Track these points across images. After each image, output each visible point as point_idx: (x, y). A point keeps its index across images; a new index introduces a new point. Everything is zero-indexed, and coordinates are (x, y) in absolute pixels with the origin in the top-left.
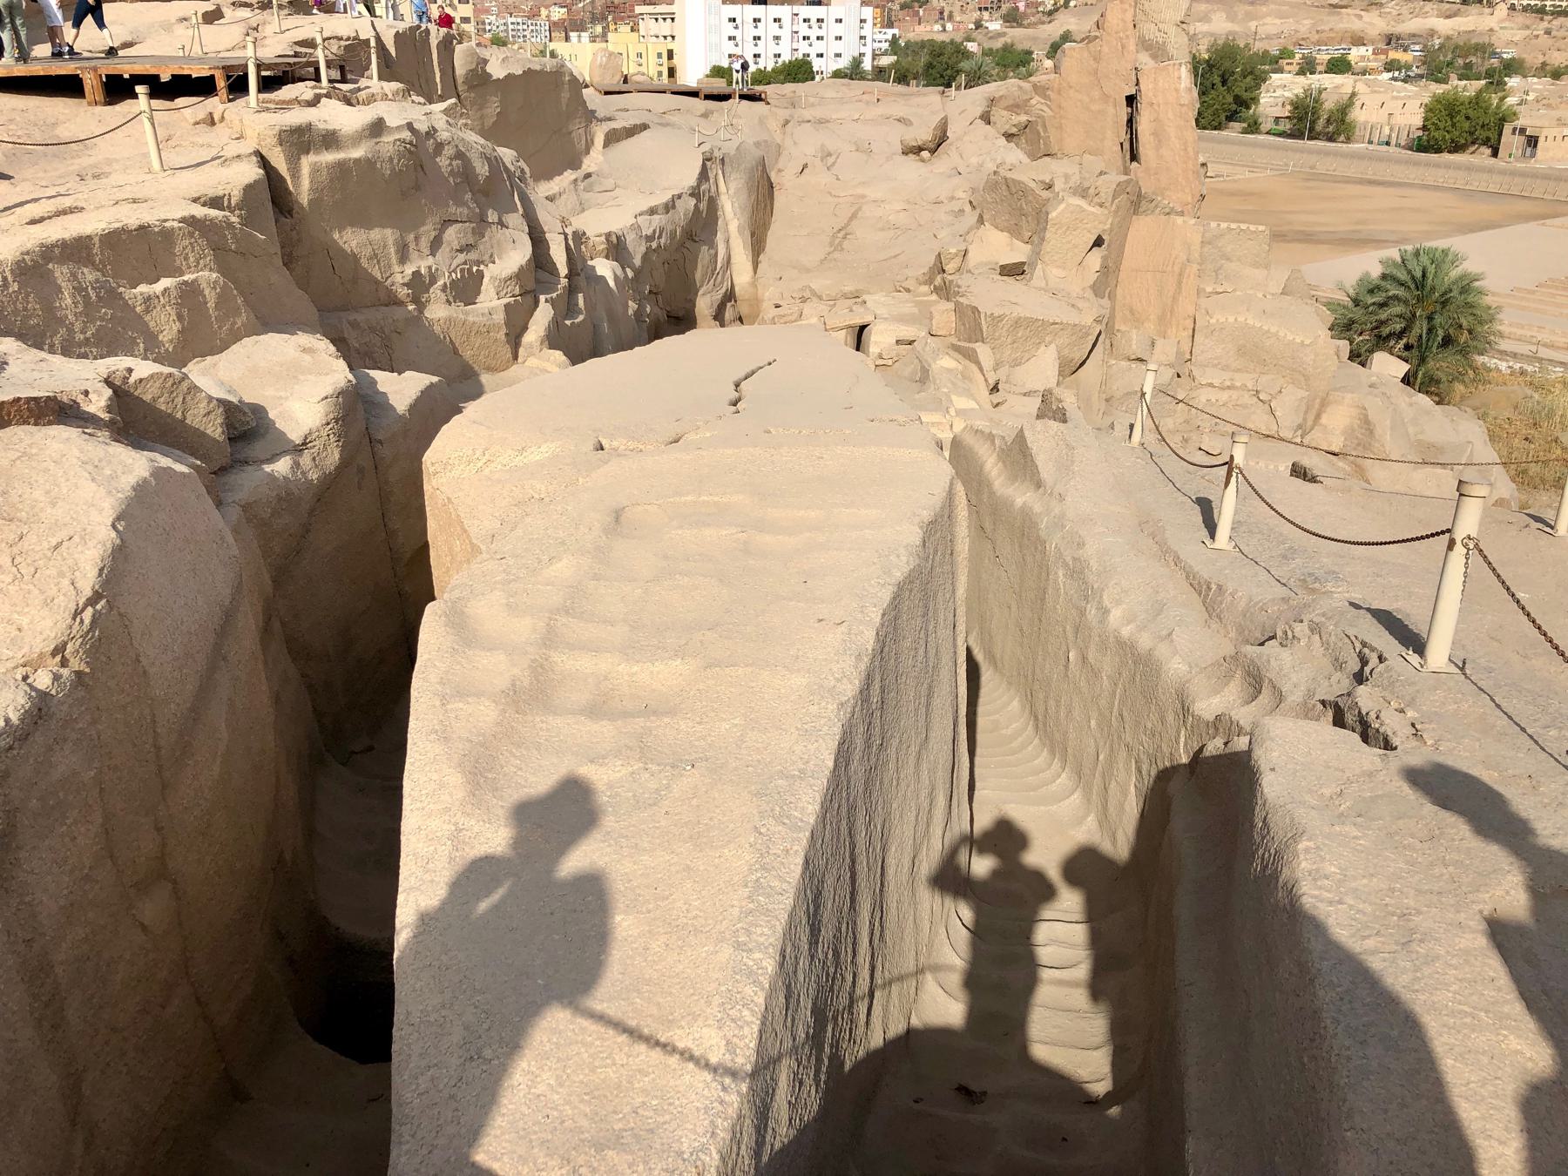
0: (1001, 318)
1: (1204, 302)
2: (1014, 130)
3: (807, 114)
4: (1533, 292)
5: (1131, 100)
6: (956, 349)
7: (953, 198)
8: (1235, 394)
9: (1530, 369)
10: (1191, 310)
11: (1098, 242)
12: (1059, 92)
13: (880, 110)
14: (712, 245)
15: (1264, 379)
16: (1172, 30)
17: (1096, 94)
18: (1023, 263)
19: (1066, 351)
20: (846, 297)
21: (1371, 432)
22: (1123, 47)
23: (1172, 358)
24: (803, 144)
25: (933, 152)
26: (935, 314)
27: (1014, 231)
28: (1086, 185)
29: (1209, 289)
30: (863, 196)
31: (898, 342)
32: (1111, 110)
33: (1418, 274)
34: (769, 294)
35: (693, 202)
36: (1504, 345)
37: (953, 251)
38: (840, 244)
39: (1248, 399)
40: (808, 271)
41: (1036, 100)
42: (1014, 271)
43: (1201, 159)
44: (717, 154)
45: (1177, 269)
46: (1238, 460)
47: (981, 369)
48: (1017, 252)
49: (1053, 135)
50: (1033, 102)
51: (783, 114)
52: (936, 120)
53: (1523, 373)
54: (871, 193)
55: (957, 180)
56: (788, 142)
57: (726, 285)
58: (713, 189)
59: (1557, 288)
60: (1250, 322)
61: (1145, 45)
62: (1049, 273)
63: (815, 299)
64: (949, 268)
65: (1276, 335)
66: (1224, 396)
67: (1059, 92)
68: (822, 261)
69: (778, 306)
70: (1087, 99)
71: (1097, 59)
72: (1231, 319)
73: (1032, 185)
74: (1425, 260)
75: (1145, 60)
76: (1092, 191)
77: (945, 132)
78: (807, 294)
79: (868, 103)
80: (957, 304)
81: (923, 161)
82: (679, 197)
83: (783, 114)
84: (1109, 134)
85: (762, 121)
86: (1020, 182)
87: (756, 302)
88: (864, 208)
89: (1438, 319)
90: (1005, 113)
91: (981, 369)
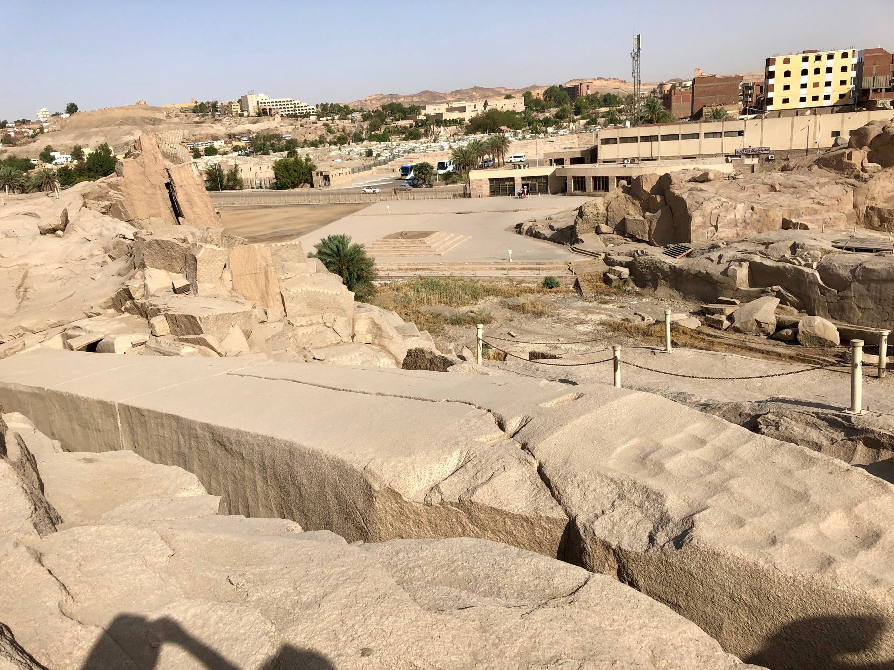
1: (283, 285)
2: (104, 210)
5: (168, 185)
6: (187, 341)
7: (92, 256)
8: (314, 327)
10: (278, 290)
12: (126, 186)
15: (325, 316)
16: (179, 147)
17: (148, 184)
18: (188, 285)
20: (51, 326)
25: (63, 230)
26: (155, 324)
27: (170, 268)
28: (205, 236)
29: (283, 278)
30: (26, 264)
33: (336, 249)
36: (381, 274)
37: (137, 286)
38: (24, 295)
39: (322, 328)
40: (11, 317)
41: (112, 192)
42: (184, 290)
43: (216, 211)
45: (263, 271)
46: (619, 358)
47: (212, 348)
49: (128, 208)
52: (60, 212)
53: (386, 285)
54: (33, 260)
55: (89, 245)
60: (309, 289)
61: (166, 156)
62: (205, 286)
63: (28, 333)
64: (136, 295)
65: (323, 293)
66: (310, 329)
67: (126, 186)
68: (18, 309)
71: (142, 165)
72: (300, 290)
74: (336, 242)
75: (168, 163)
76: (209, 239)
77: (67, 217)
78: (21, 332)
80: (166, 315)
81: (59, 236)
84: (161, 204)
86: (167, 241)
89: (351, 268)
91: (212, 348)
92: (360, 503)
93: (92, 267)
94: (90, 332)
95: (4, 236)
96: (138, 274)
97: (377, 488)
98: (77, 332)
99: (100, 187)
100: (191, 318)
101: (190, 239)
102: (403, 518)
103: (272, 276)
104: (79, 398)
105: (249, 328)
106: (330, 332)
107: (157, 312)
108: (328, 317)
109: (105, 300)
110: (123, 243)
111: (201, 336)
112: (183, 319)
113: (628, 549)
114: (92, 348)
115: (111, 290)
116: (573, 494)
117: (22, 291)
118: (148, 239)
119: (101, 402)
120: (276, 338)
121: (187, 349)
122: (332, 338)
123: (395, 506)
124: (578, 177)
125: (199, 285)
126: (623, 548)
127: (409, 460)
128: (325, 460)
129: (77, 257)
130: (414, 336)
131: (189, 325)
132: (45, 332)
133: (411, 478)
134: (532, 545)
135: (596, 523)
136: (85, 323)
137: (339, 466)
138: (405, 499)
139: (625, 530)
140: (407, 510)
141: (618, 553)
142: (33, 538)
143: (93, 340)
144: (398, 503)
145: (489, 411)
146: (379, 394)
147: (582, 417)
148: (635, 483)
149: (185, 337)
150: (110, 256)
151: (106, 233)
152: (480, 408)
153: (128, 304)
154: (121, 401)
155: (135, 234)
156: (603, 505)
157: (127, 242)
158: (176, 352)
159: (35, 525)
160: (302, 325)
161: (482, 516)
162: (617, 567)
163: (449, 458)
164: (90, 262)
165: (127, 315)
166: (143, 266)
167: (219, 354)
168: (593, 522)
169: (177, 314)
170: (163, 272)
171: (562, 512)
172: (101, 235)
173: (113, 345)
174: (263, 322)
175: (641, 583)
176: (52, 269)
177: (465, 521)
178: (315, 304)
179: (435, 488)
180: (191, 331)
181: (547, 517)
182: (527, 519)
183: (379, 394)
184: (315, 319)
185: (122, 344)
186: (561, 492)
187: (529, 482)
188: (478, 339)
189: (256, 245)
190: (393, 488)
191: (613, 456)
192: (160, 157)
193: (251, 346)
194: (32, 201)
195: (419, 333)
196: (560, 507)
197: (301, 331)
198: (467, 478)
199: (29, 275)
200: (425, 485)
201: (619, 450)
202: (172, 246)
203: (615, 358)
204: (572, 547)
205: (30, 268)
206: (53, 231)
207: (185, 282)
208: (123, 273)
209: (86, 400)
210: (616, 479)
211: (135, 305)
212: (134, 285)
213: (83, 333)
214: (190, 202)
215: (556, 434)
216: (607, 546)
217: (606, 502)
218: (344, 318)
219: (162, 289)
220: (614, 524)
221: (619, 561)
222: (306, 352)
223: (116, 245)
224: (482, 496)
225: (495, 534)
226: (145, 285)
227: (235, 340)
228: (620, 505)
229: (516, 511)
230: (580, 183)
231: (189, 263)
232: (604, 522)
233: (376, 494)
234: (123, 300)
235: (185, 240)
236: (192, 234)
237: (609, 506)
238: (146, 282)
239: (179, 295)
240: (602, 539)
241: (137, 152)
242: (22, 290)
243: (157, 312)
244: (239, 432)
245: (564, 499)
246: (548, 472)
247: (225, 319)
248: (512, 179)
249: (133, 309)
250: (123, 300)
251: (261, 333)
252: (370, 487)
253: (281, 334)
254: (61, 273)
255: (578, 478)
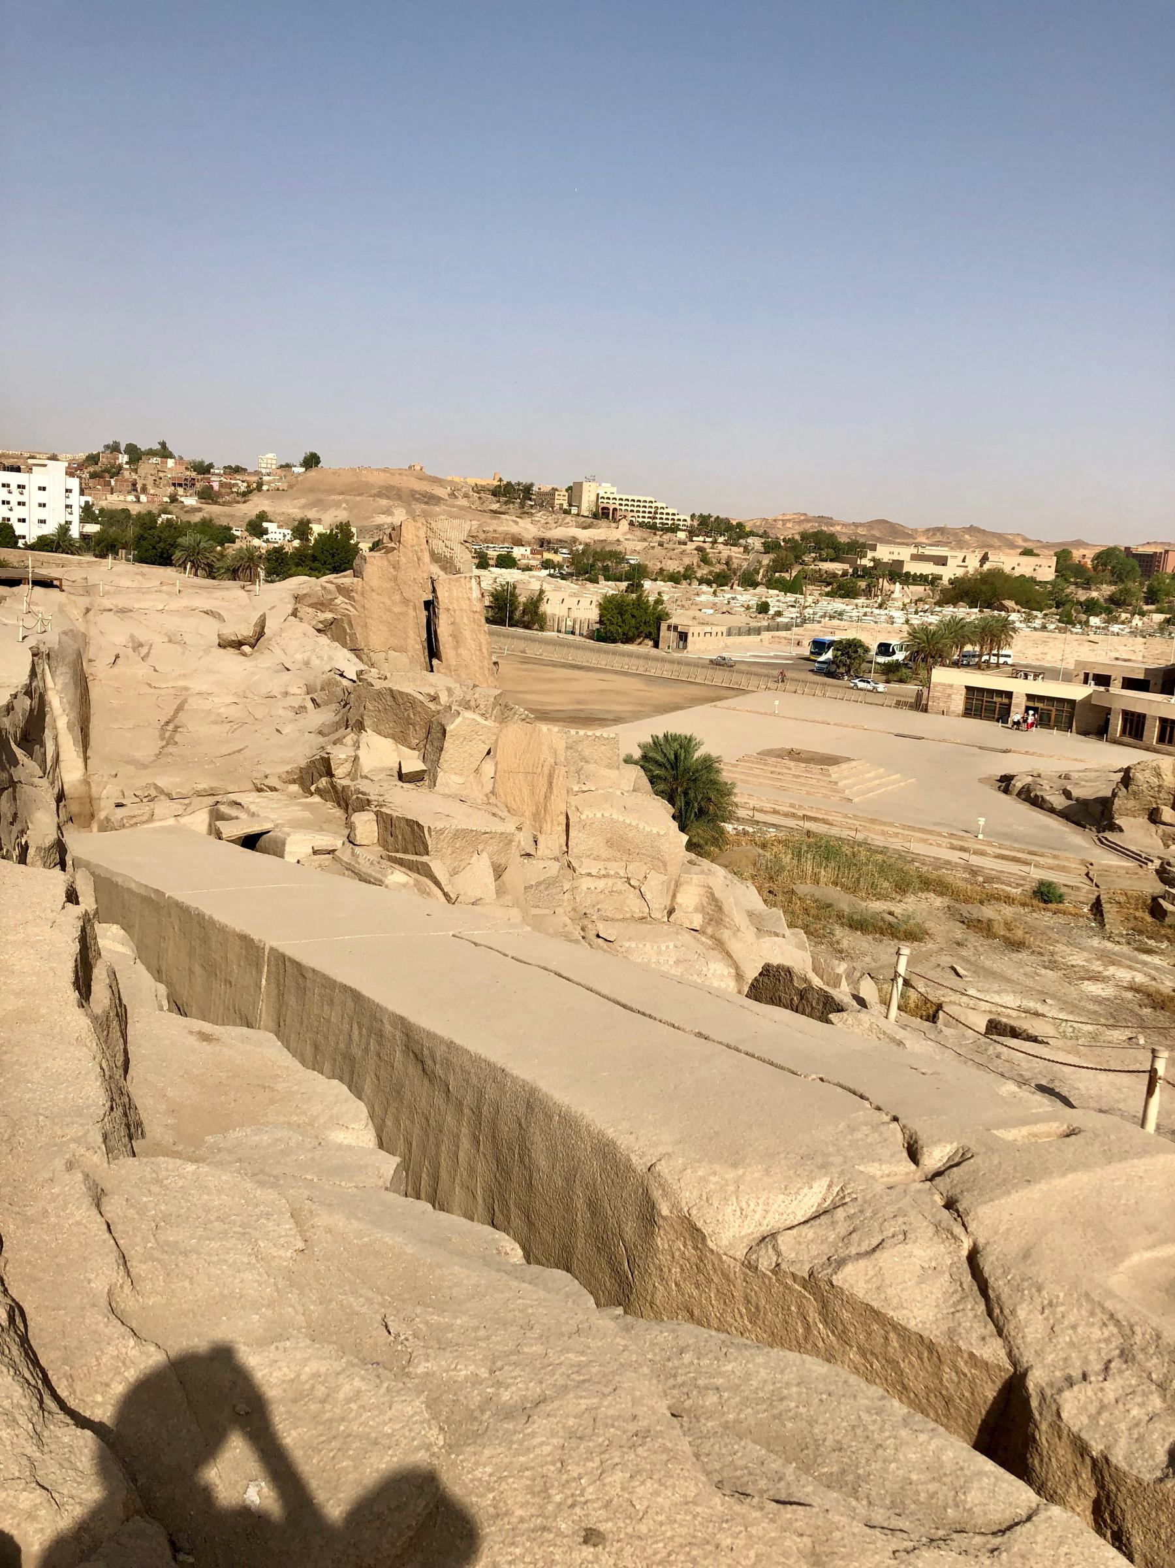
0: (442, 831)
1: (574, 800)
2: (321, 626)
3: (107, 603)
4: (736, 766)
5: (429, 605)
6: (401, 863)
7: (286, 694)
8: (610, 882)
9: (751, 830)
11: (488, 753)
12: (362, 594)
13: (177, 604)
14: (42, 744)
15: (631, 867)
17: (397, 597)
18: (424, 771)
19: (495, 858)
21: (720, 909)
22: (419, 559)
23: (557, 853)
24: (110, 635)
25: (253, 646)
27: (401, 738)
29: (576, 788)
30: (186, 689)
31: (315, 852)
32: (412, 613)
33: (673, 757)
34: (107, 793)
35: (28, 702)
37: (343, 756)
38: (172, 737)
39: (621, 885)
40: (145, 767)
41: (340, 600)
43: (494, 659)
44: (43, 649)
45: (546, 772)
46: (1161, 1072)
47: (437, 884)
48: (413, 763)
49: (358, 630)
50: (338, 601)
51: (83, 602)
52: (255, 617)
53: (745, 833)
54: (196, 685)
55: (287, 676)
56: (93, 632)
57: (58, 785)
58: (41, 685)
59: (753, 762)
61: (435, 558)
62: (449, 778)
63: (162, 797)
64: (339, 772)
65: (637, 827)
66: (601, 884)
67: (362, 594)
69: (119, 805)
70: (389, 602)
71: (396, 566)
72: (599, 815)
73: (421, 697)
74: (676, 746)
75: (436, 570)
76: (473, 703)
78: (153, 793)
79: (169, 594)
80: (377, 814)
81: (245, 655)
82: (15, 696)
83: (83, 602)
84: (411, 634)
85: (61, 609)
86: (407, 695)
87: (90, 800)
88: (190, 700)
89: (691, 794)
90: (310, 610)
91: (437, 884)
92: (630, 1229)
93: (281, 712)
94: (253, 815)
95: (166, 640)
96: (350, 738)
97: (665, 1212)
98: (233, 812)
99: (324, 588)
100: (415, 827)
101: (444, 699)
102: (701, 1278)
103: (559, 782)
104: (212, 922)
105: (503, 861)
106: (633, 895)
107: (364, 804)
108: (636, 869)
109: (288, 768)
110: (337, 684)
111: (425, 859)
112: (403, 824)
113: (1123, 1465)
114: (250, 842)
115: (301, 755)
116: (1029, 1324)
117: (170, 729)
118: (378, 685)
119: (245, 939)
120: (542, 887)
121: (398, 876)
122: (635, 906)
123: (690, 1252)
124: (1133, 714)
125: (440, 774)
126: (1113, 1460)
127: (731, 1175)
128: (584, 1134)
129: (264, 691)
130: (777, 935)
131: (409, 836)
132: (186, 801)
133: (729, 1210)
134: (933, 1399)
135: (1067, 1394)
136: (249, 798)
137: (606, 1151)
138: (709, 1243)
139: (1123, 1426)
140: (709, 1267)
141: (1100, 1468)
142: (97, 1159)
143: (255, 829)
144: (696, 1248)
145: (895, 1119)
146: (699, 1035)
147: (1070, 1176)
148: (1159, 1337)
149: (399, 855)
150: (313, 700)
151: (315, 662)
152: (879, 1109)
153: (323, 782)
154: (275, 944)
155: (360, 673)
156: (1086, 1361)
157: (345, 682)
158: (379, 876)
159: (105, 1137)
160: (589, 875)
161: (846, 1315)
162: (1093, 1494)
163: (806, 1190)
164: (281, 704)
165: (316, 799)
166: (360, 727)
167: (446, 894)
168: (1060, 1391)
169: (395, 814)
170: (388, 743)
171: (1002, 1353)
172: (307, 664)
173: (284, 844)
174: (528, 855)
175: (1137, 1541)
176: (222, 703)
177: (813, 1316)
178: (619, 844)
179: (769, 1238)
180: (410, 847)
181: (971, 1355)
182: (931, 1347)
183: (699, 1035)
184: (615, 867)
185: (298, 845)
186: (1007, 1312)
187: (947, 1277)
188: (897, 974)
189: (544, 728)
190: (694, 1218)
191: (1121, 1268)
192: (426, 558)
193: (500, 891)
194: (218, 594)
195: (788, 932)
196: (1000, 1341)
197: (586, 884)
198: (832, 1237)
199: (186, 707)
200: (752, 1228)
201: (1135, 1259)
202: (411, 702)
203: (1153, 1072)
204: (1008, 1430)
205: (192, 695)
206: (238, 645)
207: (419, 766)
208: (326, 731)
209: (223, 930)
210: (1120, 1316)
211: (334, 787)
212: (340, 755)
213: (243, 816)
214: (456, 637)
215: (1015, 1196)
216: (1081, 1448)
217: (1093, 1357)
218: (663, 878)
219: (382, 770)
220: (1102, 1408)
221: (1100, 1485)
222: (586, 922)
223: (327, 685)
224: (854, 1279)
225: (864, 1356)
226: (356, 759)
227: (476, 877)
228: (1121, 1372)
229: (912, 1325)
230: (1135, 725)
231: (433, 737)
232: (1082, 1397)
233: (661, 1222)
234: (317, 775)
235: (434, 699)
236: (449, 690)
237: (1099, 1367)
238: (360, 753)
239: (405, 785)
240: (1075, 1429)
241: (392, 545)
242: (171, 727)
243: (364, 804)
244: (451, 1045)
245: (1010, 1328)
246: (988, 1266)
247: (469, 840)
248: (1009, 695)
249: (329, 792)
250: (317, 775)
251: (520, 874)
252: (653, 1207)
253: (550, 883)
254: (233, 712)
255: (1044, 1293)
